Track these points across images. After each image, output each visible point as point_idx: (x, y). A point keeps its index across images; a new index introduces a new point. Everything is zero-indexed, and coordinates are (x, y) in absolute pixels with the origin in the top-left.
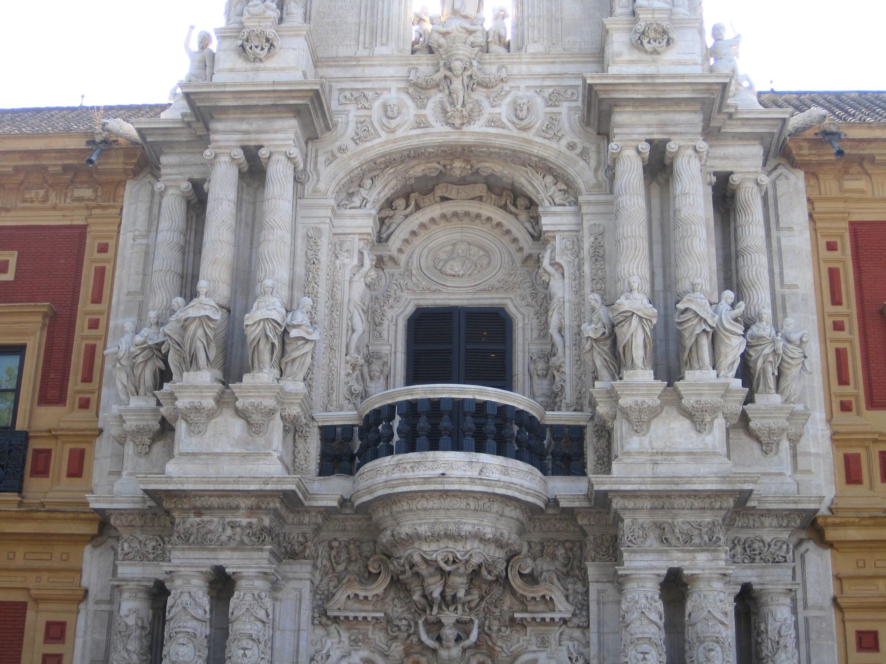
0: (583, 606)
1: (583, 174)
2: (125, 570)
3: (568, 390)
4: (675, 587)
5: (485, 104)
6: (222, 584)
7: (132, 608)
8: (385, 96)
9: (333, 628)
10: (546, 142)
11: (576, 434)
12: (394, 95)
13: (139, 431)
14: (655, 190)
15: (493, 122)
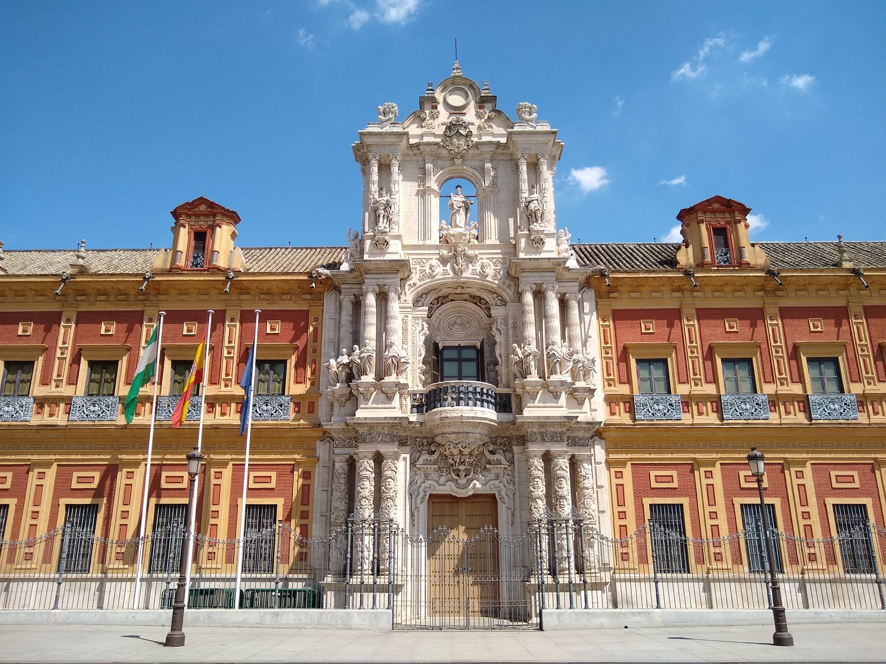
0: (512, 462)
1: (508, 294)
2: (337, 451)
3: (504, 379)
4: (547, 458)
6: (379, 459)
7: (340, 466)
8: (430, 262)
9: (418, 472)
11: (508, 396)
12: (434, 262)
13: (341, 396)
14: (537, 301)
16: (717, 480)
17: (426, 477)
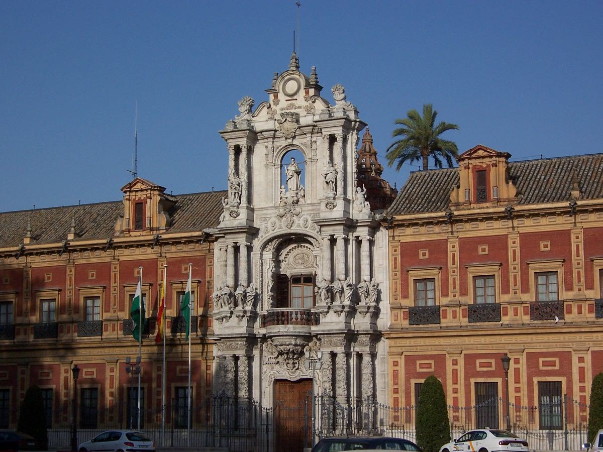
5: (296, 220)
10: (311, 231)
15: (299, 226)
16: (461, 367)
17: (272, 368)
